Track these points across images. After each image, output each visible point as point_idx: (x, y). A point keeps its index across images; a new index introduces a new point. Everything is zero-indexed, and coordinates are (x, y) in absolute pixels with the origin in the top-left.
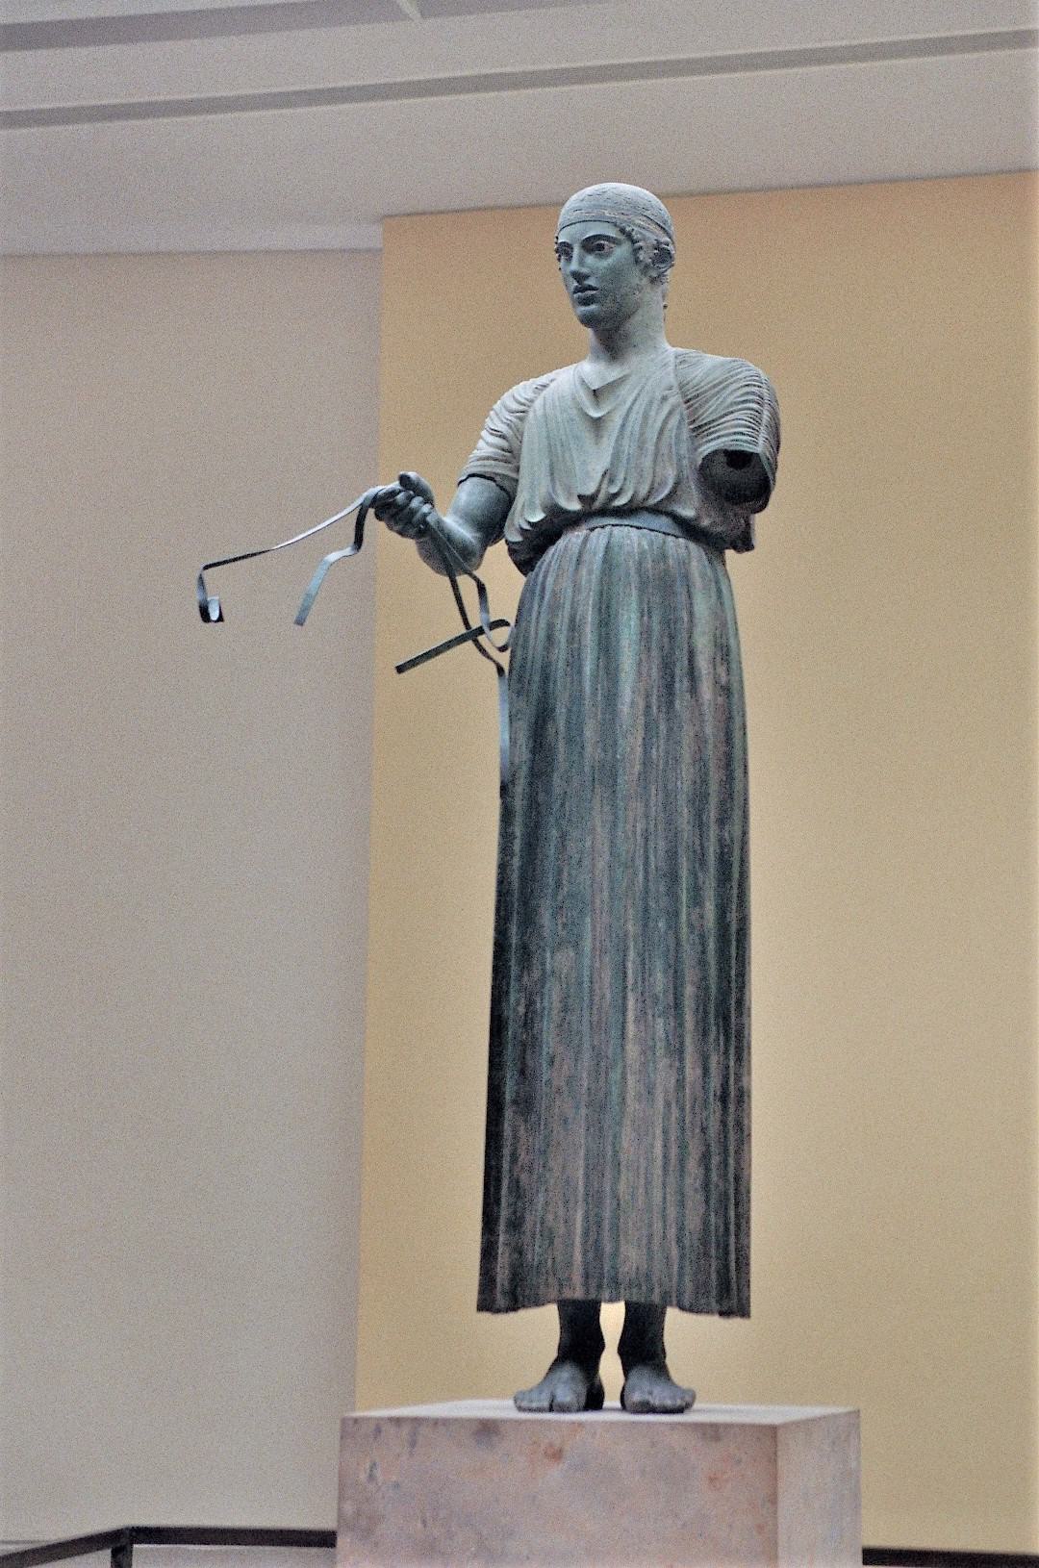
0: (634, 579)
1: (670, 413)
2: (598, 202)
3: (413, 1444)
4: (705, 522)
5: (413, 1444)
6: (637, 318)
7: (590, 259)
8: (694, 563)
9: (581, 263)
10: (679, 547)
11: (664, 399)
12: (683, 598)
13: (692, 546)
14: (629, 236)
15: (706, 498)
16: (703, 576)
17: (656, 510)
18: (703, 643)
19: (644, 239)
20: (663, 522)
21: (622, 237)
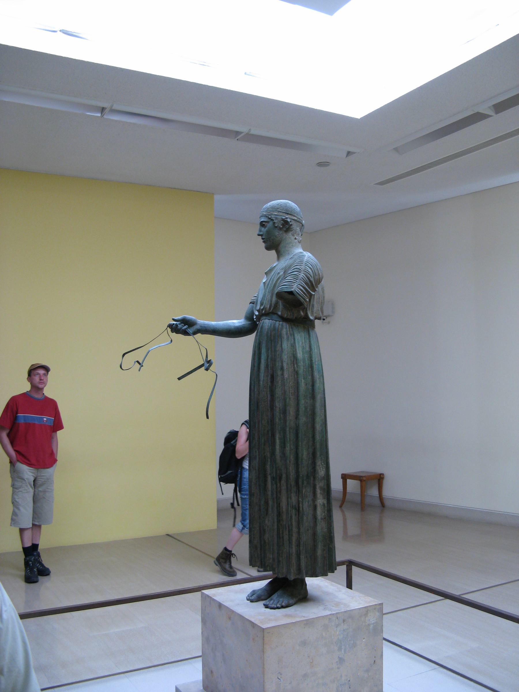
0: (266, 338)
1: (279, 278)
2: (274, 209)
3: (210, 603)
4: (285, 316)
5: (210, 603)
6: (282, 245)
7: (263, 229)
8: (284, 330)
9: (260, 231)
10: (278, 324)
11: (279, 273)
12: (280, 343)
13: (284, 324)
14: (272, 220)
15: (284, 306)
16: (287, 334)
17: (273, 313)
18: (285, 357)
19: (276, 218)
20: (275, 317)
21: (269, 220)
